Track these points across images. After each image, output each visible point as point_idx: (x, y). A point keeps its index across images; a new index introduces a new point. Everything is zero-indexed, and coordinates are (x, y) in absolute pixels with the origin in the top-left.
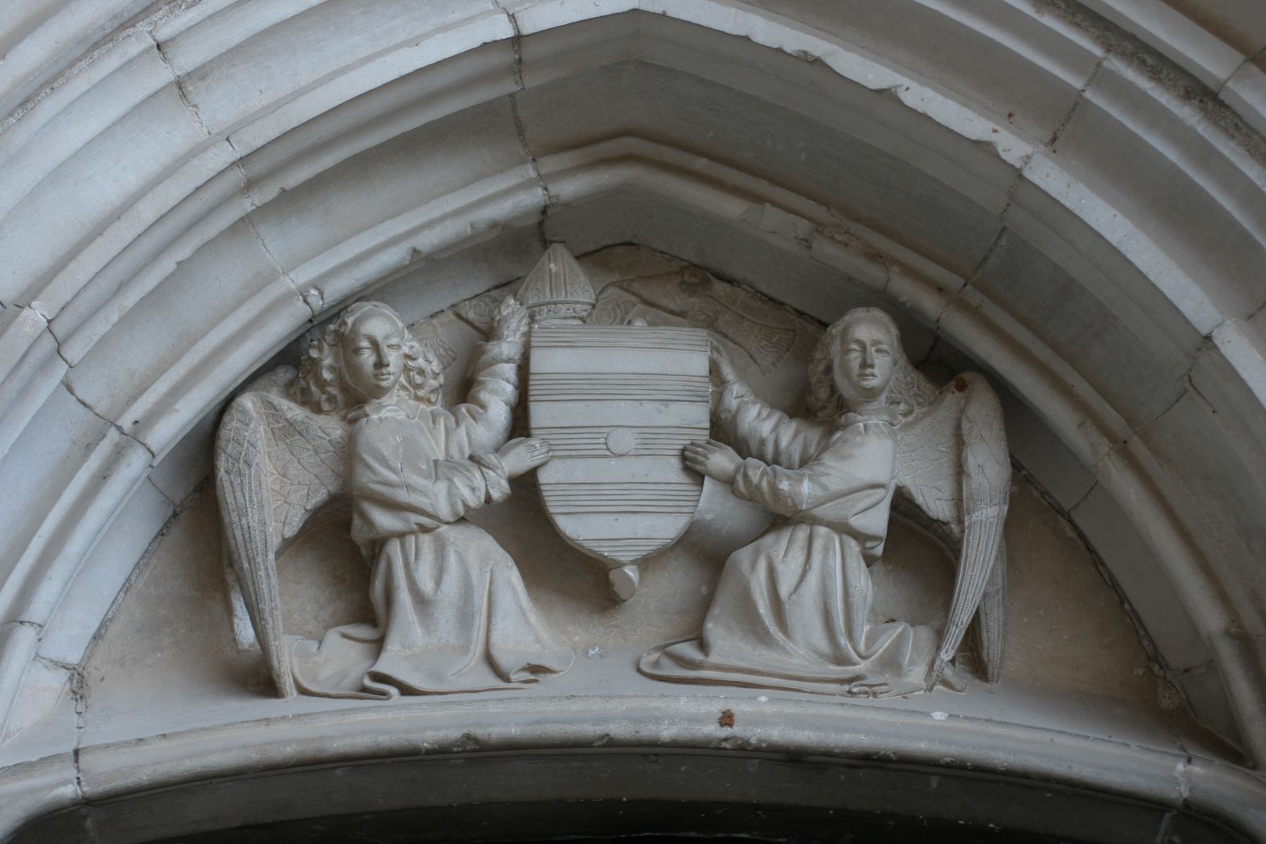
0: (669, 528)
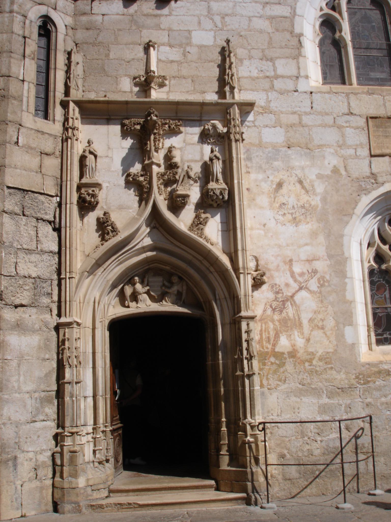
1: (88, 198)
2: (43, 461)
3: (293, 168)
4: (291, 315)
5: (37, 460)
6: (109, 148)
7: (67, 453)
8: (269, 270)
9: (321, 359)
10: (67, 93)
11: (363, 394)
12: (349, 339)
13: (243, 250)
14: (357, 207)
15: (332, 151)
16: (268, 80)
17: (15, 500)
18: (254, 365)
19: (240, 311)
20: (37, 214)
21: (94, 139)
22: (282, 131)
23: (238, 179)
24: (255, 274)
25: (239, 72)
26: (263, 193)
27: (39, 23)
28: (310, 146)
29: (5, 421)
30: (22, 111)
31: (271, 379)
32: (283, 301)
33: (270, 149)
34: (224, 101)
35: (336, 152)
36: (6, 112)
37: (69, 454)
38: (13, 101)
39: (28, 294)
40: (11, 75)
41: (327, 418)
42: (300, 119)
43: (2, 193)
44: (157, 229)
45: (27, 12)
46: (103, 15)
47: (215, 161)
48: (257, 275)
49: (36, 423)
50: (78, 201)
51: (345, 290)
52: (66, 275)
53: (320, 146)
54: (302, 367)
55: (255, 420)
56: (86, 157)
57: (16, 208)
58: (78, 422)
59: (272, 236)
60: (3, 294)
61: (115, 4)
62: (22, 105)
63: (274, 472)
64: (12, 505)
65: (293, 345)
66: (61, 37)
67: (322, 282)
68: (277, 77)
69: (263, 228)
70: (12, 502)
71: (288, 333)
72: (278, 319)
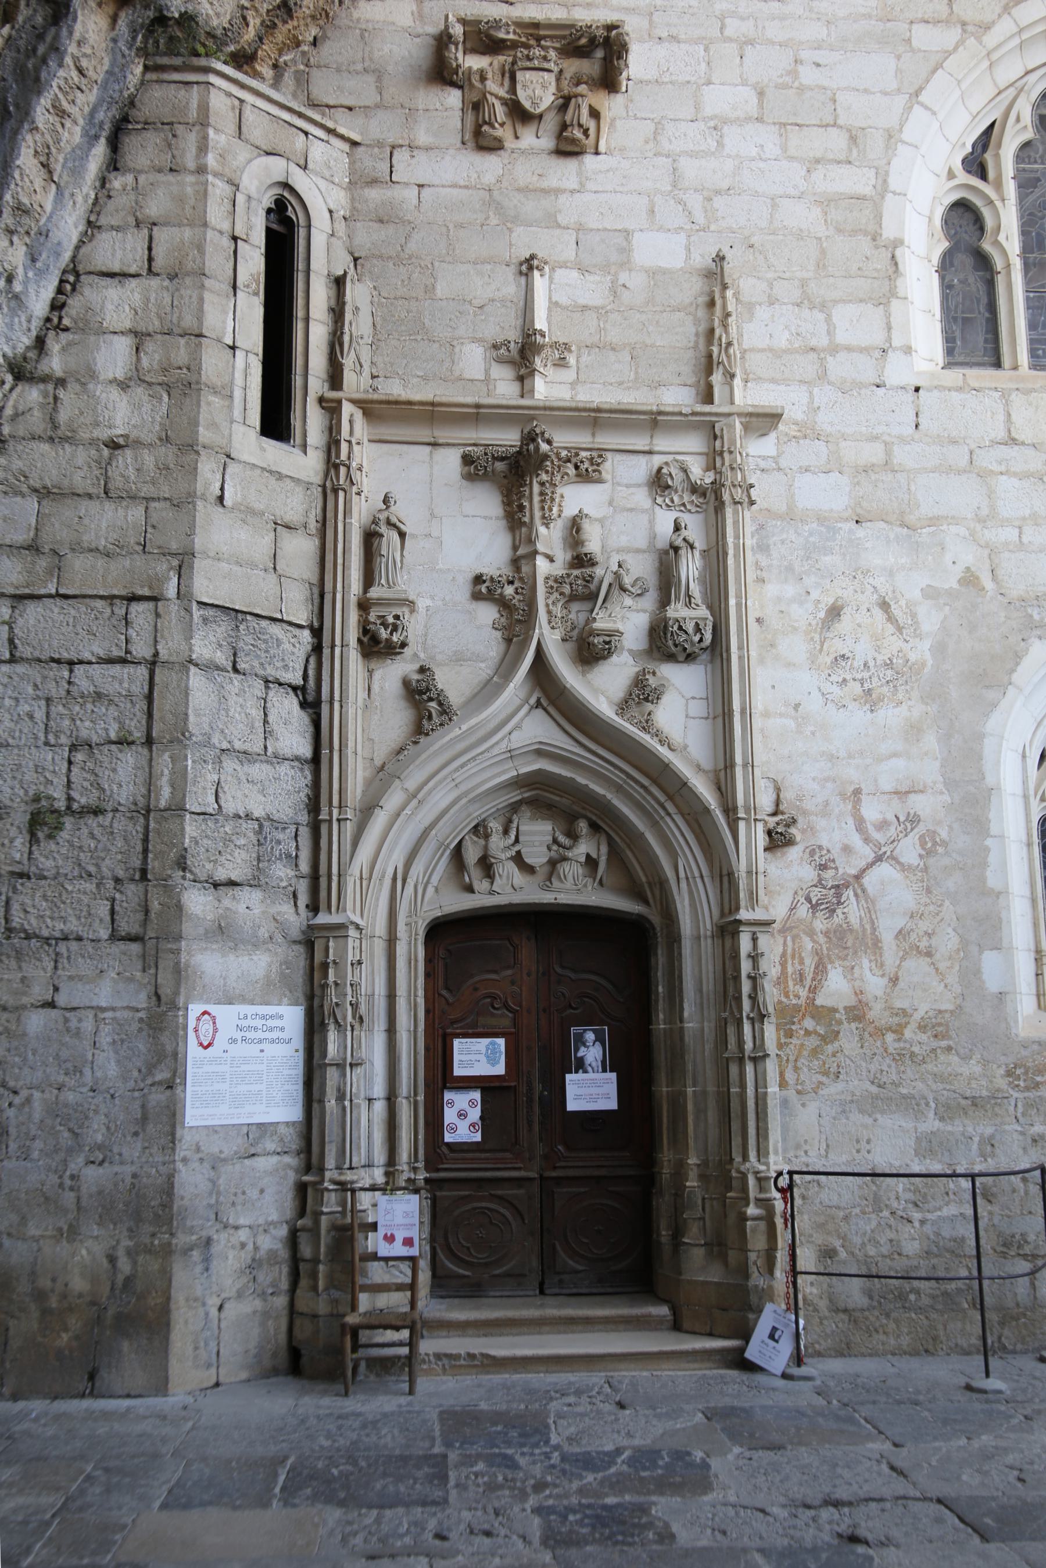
0: (545, 860)
1: (384, 634)
2: (271, 1250)
3: (868, 571)
4: (854, 921)
5: (256, 1248)
6: (432, 515)
7: (329, 1231)
8: (805, 813)
9: (925, 1027)
10: (335, 378)
11: (1024, 1114)
12: (992, 983)
13: (745, 765)
14: (1019, 668)
15: (963, 531)
16: (813, 356)
17: (202, 1344)
18: (766, 1034)
19: (738, 909)
20: (265, 669)
21: (396, 494)
22: (844, 480)
23: (738, 597)
24: (772, 821)
25: (745, 337)
26: (795, 629)
27: (268, 201)
28: (911, 519)
29: (188, 1154)
30: (232, 422)
31: (805, 1070)
32: (837, 887)
33: (814, 525)
34: (707, 408)
35: (973, 533)
36: (194, 423)
37: (333, 1233)
38: (211, 398)
39: (244, 855)
40: (205, 332)
41: (936, 1168)
42: (888, 453)
43: (187, 617)
44: (545, 709)
46: (420, 186)
47: (682, 552)
48: (778, 824)
49: (256, 1159)
50: (359, 640)
51: (984, 865)
52: (331, 814)
53: (934, 521)
54: (879, 1044)
55: (767, 1164)
56: (382, 536)
57: (219, 654)
58: (354, 1159)
59: (813, 733)
60: (189, 856)
61: (448, 158)
62: (230, 407)
63: (808, 1290)
64: (196, 1357)
65: (859, 993)
66: (319, 240)
67: (929, 845)
68: (834, 349)
69: (793, 712)
70: (196, 1348)
71: (846, 963)
72: (824, 929)
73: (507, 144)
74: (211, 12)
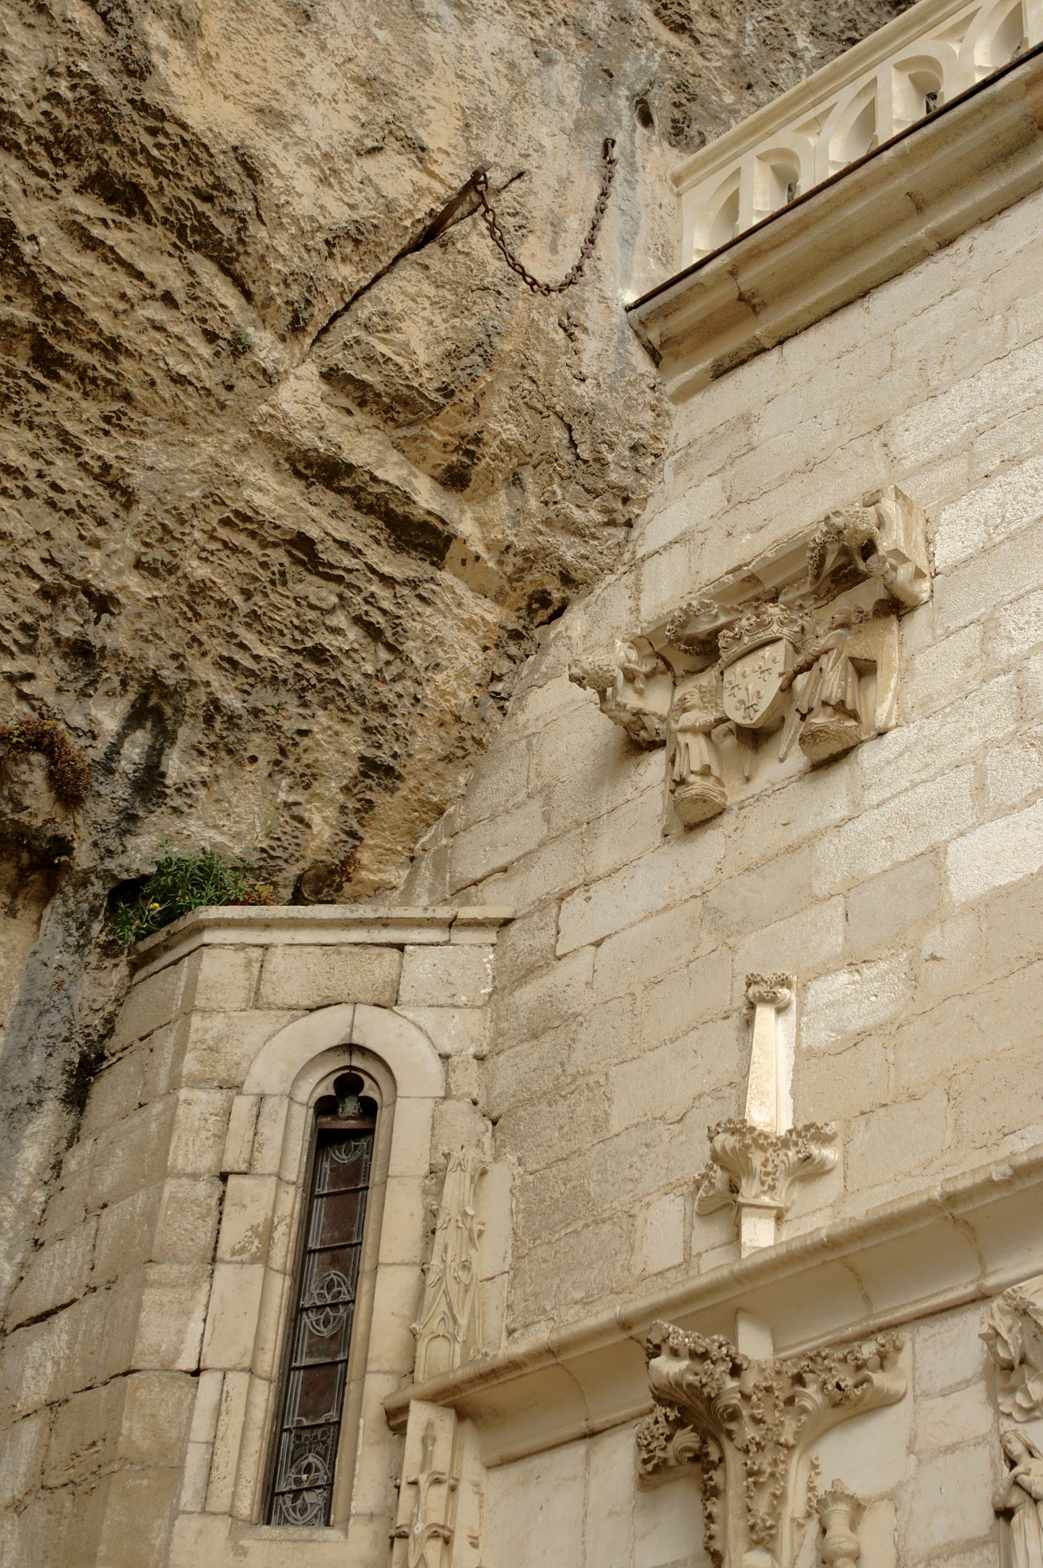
45: (245, 1064)
46: (598, 944)
73: (732, 800)
74: (219, 838)
